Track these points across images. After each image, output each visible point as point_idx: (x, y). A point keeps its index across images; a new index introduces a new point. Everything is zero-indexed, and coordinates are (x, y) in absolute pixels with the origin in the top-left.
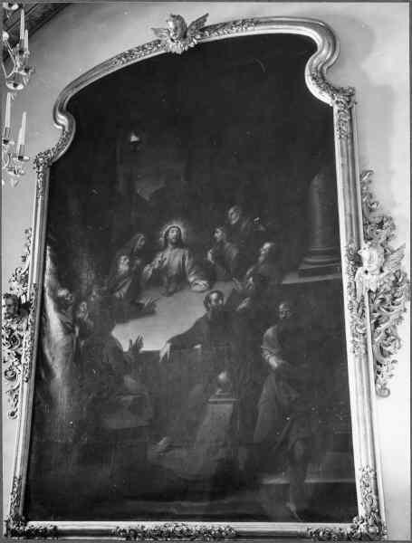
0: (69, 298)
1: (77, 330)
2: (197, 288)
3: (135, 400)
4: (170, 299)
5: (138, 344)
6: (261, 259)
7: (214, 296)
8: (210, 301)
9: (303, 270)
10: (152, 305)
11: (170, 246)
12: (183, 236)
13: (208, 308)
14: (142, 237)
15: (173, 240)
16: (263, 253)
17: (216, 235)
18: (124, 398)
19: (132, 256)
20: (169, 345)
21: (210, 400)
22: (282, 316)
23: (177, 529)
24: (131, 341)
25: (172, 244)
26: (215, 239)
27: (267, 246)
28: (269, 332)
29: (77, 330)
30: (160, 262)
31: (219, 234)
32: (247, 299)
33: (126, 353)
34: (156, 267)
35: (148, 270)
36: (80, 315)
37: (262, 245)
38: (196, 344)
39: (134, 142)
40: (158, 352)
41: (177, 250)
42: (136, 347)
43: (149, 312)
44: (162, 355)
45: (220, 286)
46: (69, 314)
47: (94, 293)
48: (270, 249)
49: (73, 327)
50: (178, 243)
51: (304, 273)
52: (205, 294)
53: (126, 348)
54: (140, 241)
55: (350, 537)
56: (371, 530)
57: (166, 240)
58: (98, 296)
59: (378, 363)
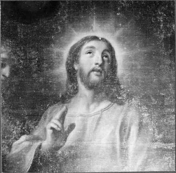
15: (94, 77)
25: (91, 87)
34: (47, 143)
41: (104, 104)
57: (72, 73)
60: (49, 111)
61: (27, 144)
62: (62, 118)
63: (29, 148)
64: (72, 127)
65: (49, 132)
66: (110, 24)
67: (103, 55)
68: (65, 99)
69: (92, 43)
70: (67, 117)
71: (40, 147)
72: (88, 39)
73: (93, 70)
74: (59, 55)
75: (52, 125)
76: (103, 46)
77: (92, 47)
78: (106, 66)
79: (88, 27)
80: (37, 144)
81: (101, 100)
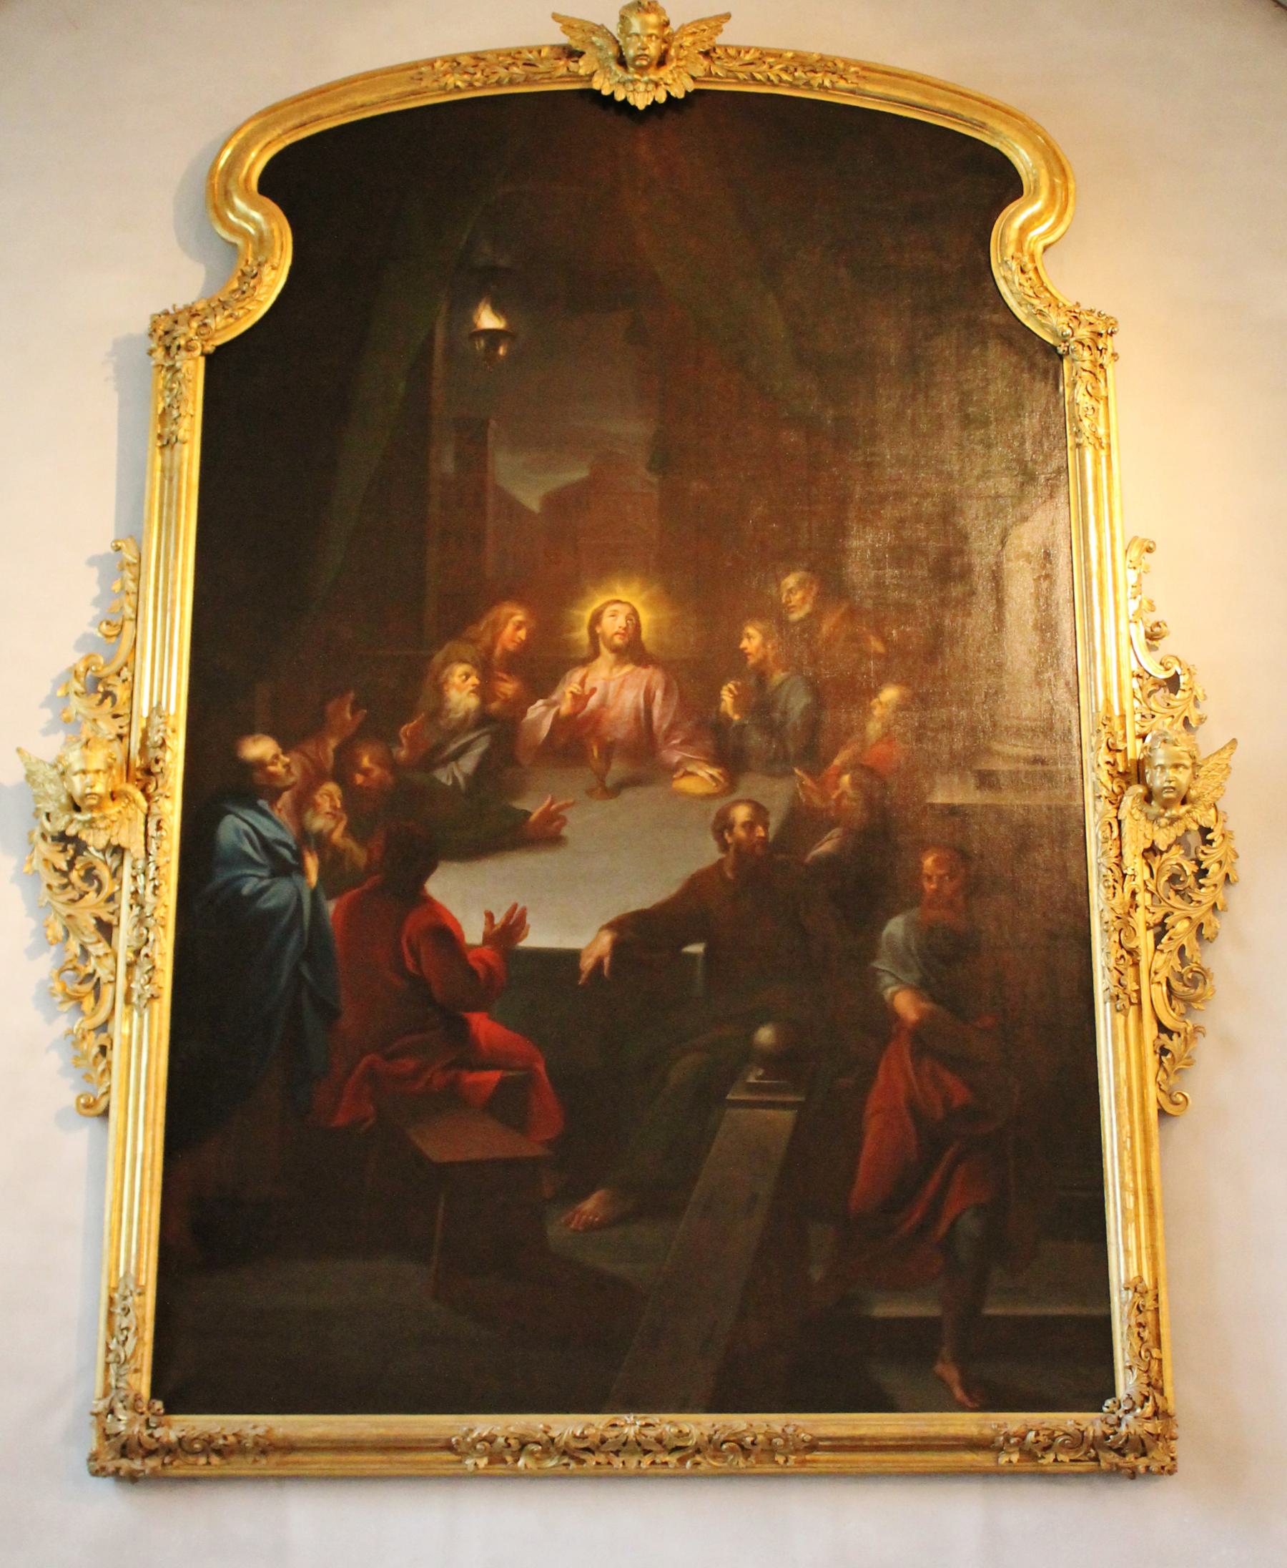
0: (278, 768)
1: (312, 864)
2: (687, 785)
3: (502, 1083)
4: (613, 804)
5: (514, 926)
7: (741, 814)
8: (730, 827)
10: (552, 816)
11: (607, 656)
12: (645, 634)
13: (724, 847)
14: (519, 617)
15: (618, 641)
18: (470, 1078)
19: (486, 670)
20: (606, 939)
21: (729, 1097)
22: (930, 887)
23: (651, 1433)
24: (490, 916)
25: (615, 650)
26: (743, 655)
28: (895, 927)
29: (312, 864)
30: (580, 699)
31: (753, 640)
32: (836, 832)
34: (565, 708)
35: (540, 716)
36: (319, 823)
38: (686, 943)
39: (492, 334)
40: (572, 957)
41: (628, 668)
44: (587, 963)
45: (756, 785)
46: (283, 817)
47: (366, 762)
49: (299, 856)
52: (717, 805)
53: (473, 933)
55: (1100, 1443)
56: (1149, 1427)
57: (594, 637)
58: (377, 772)
59: (1162, 1028)
60: (568, 675)
61: (543, 709)
62: (582, 683)
63: (545, 714)
64: (593, 690)
65: (569, 696)
66: (635, 586)
67: (627, 618)
68: (585, 662)
70: (587, 680)
71: (558, 713)
72: (609, 603)
73: (617, 633)
74: (580, 619)
76: (626, 610)
77: (615, 611)
78: (631, 631)
79: (611, 591)
80: (553, 711)
81: (626, 663)
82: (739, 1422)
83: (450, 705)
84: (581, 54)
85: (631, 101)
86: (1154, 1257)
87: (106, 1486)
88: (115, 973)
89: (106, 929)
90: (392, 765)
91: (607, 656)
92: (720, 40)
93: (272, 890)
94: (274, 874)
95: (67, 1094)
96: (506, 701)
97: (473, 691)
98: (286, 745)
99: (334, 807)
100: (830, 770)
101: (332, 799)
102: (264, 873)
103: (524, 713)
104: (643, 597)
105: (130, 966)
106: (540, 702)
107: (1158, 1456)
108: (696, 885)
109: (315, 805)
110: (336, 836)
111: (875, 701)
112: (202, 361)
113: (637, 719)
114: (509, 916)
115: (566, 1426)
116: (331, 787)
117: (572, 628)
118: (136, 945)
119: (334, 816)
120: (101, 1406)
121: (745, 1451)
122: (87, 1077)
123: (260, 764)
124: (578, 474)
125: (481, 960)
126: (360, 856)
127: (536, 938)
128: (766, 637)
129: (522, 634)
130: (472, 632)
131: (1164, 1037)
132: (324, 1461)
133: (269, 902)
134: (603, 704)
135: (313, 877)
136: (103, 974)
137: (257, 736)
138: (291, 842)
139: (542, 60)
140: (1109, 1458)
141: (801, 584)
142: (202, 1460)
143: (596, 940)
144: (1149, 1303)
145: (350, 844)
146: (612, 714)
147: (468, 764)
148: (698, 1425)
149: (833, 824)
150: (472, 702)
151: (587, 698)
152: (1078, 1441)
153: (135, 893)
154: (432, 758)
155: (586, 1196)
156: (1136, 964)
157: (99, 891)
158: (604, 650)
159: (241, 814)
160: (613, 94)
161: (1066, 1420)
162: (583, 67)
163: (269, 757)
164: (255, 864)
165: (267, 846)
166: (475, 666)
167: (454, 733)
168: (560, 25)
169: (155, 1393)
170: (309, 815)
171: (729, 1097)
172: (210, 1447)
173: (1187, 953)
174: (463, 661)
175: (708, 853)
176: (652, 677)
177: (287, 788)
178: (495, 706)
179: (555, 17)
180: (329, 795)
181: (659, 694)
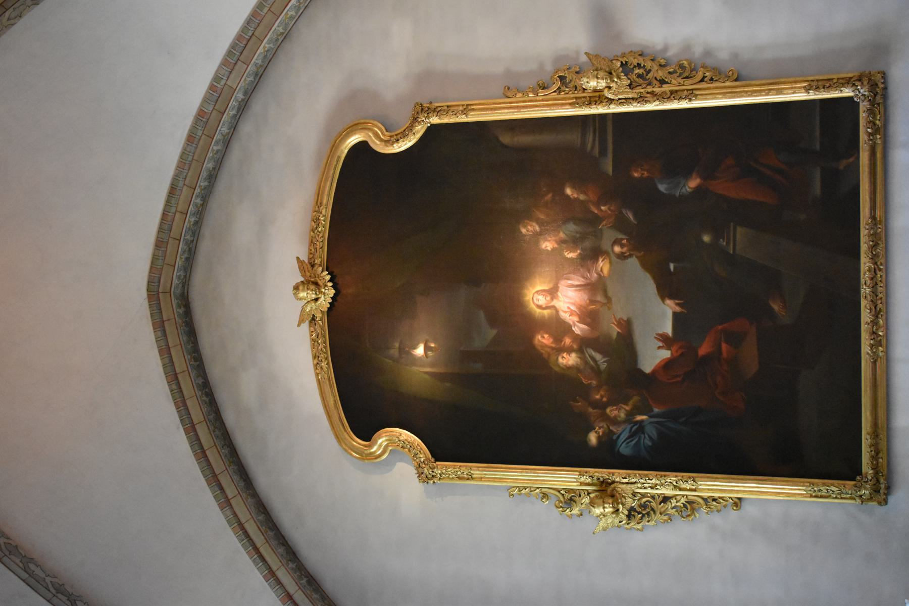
0: (601, 431)
1: (639, 418)
3: (727, 342)
4: (614, 299)
5: (664, 338)
6: (582, 197)
7: (617, 249)
8: (622, 253)
9: (600, 152)
10: (619, 323)
11: (555, 303)
12: (546, 288)
13: (631, 256)
15: (548, 298)
16: (576, 196)
17: (549, 248)
19: (560, 350)
20: (668, 302)
21: (732, 252)
22: (646, 174)
23: (868, 282)
25: (552, 299)
26: (553, 249)
27: (569, 191)
28: (662, 187)
29: (639, 418)
30: (572, 313)
32: (624, 211)
33: (672, 354)
34: (576, 319)
36: (623, 415)
37: (568, 196)
38: (669, 269)
39: (427, 348)
40: (675, 315)
41: (559, 294)
42: (666, 341)
43: (627, 326)
44: (678, 309)
45: (606, 244)
46: (620, 429)
47: (598, 397)
48: (573, 187)
49: (637, 422)
50: (553, 293)
51: (603, 152)
52: (614, 258)
53: (666, 354)
54: (543, 340)
55: (872, 103)
56: (865, 83)
57: (547, 308)
58: (602, 393)
59: (702, 80)
60: (562, 318)
61: (576, 327)
62: (566, 312)
63: (578, 326)
64: (568, 308)
65: (571, 317)
66: (526, 291)
68: (557, 311)
69: (535, 299)
70: (564, 310)
71: (578, 322)
72: (533, 302)
74: (539, 313)
75: (568, 316)
76: (536, 295)
77: (536, 299)
78: (544, 293)
79: (529, 301)
81: (557, 295)
82: (864, 247)
83: (575, 363)
84: (313, 315)
85: (332, 295)
86: (796, 82)
87: (891, 499)
88: (683, 496)
89: (666, 499)
90: (599, 388)
91: (555, 303)
92: (306, 261)
93: (650, 434)
94: (644, 433)
95: (733, 514)
96: (573, 342)
97: (569, 355)
98: (591, 428)
99: (616, 409)
100: (600, 214)
101: (613, 410)
102: (643, 436)
103: (578, 335)
104: (531, 289)
105: (681, 489)
106: (573, 329)
107: (878, 78)
108: (645, 266)
109: (615, 417)
110: (627, 408)
111: (571, 197)
112: (437, 463)
113: (580, 290)
114: (660, 340)
115: (866, 316)
116: (608, 410)
117: (543, 317)
118: (672, 487)
119: (620, 409)
120: (858, 501)
121: (876, 245)
122: (725, 506)
123: (599, 438)
124: (482, 315)
125: (677, 351)
126: (636, 399)
127: (668, 330)
128: (546, 240)
129: (546, 336)
130: (545, 356)
131: (706, 79)
132: (881, 413)
133: (654, 434)
134: (574, 304)
135: (644, 417)
136: (683, 500)
137: (588, 440)
138: (629, 426)
139: (315, 330)
140: (879, 99)
141: (525, 227)
142: (880, 460)
143: (668, 305)
144: (815, 84)
145: (631, 402)
146: (578, 300)
147: (598, 357)
148: (865, 263)
149: (621, 213)
150: (573, 355)
151: (572, 310)
152: (871, 112)
153: (652, 488)
154: (596, 371)
155: (773, 309)
156: (676, 91)
157: (650, 502)
158: (552, 304)
159: (619, 447)
160: (329, 303)
161: (863, 115)
162: (319, 316)
163: (596, 435)
164: (639, 439)
165: (632, 436)
166: (559, 354)
167: (586, 363)
168: (302, 324)
169: (853, 479)
170: (619, 419)
171: (732, 252)
172: (875, 457)
173: (671, 70)
174: (557, 359)
175: (633, 263)
176: (563, 284)
177: (609, 427)
178: (575, 346)
179: (299, 326)
180: (611, 411)
181: (570, 282)
